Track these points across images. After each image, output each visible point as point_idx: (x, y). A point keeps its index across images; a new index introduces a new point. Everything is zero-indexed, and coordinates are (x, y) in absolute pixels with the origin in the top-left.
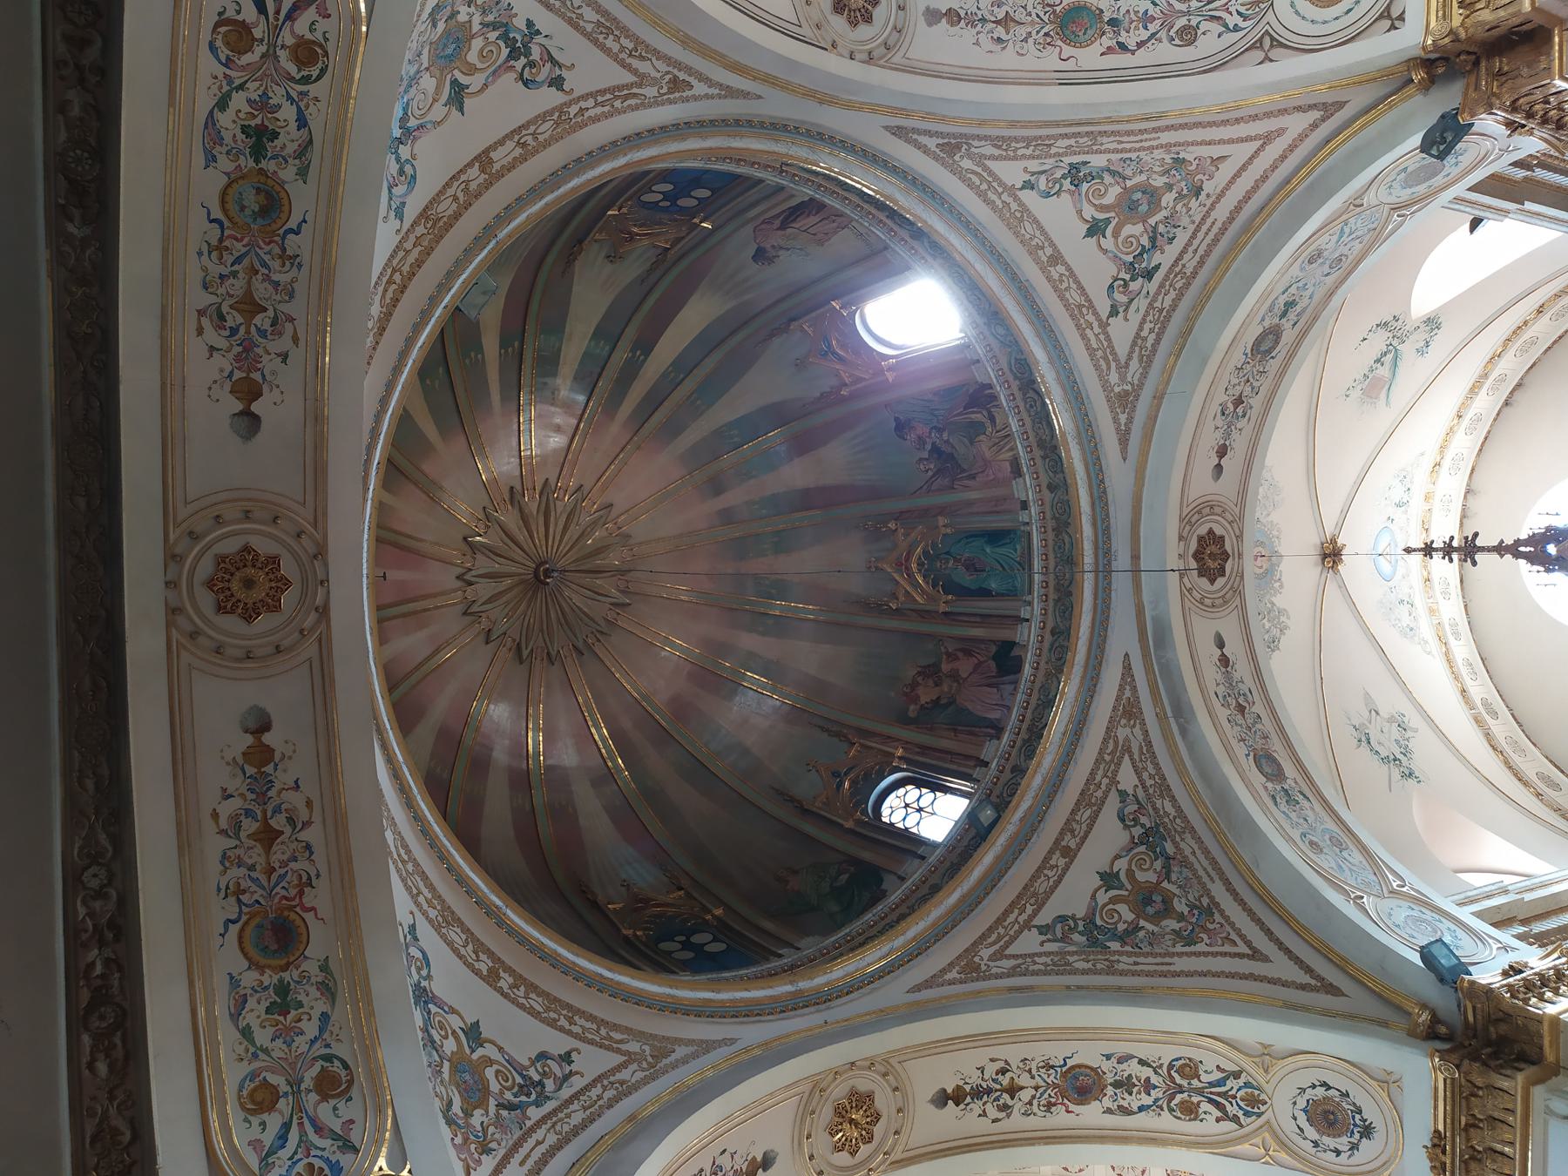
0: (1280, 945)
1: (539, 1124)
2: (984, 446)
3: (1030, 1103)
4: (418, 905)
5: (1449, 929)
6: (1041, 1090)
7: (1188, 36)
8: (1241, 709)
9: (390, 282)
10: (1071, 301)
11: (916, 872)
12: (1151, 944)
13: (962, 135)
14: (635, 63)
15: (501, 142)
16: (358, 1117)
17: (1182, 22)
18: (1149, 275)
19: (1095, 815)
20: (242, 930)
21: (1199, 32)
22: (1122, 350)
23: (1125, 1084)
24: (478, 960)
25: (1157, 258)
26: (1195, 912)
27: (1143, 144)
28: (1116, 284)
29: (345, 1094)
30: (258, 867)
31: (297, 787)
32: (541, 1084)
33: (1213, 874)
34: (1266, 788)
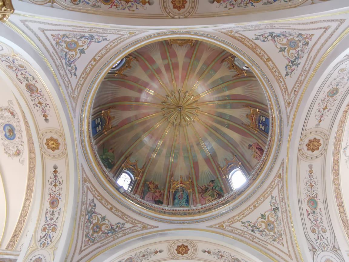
1: (61, 61)
2: (210, 198)
3: (52, 190)
4: (110, 43)
6: (54, 193)
7: (313, 231)
8: (144, 256)
9: (242, 38)
10: (245, 212)
11: (110, 175)
12: (86, 226)
13: (283, 178)
14: (293, 92)
15: (273, 63)
17: (316, 229)
18: (253, 231)
19: (120, 217)
21: (315, 233)
22: (234, 225)
23: (53, 213)
24: (98, 56)
25: (257, 232)
26: (93, 239)
27: (285, 225)
31: (137, 9)
32: (70, 66)
34: (123, 260)
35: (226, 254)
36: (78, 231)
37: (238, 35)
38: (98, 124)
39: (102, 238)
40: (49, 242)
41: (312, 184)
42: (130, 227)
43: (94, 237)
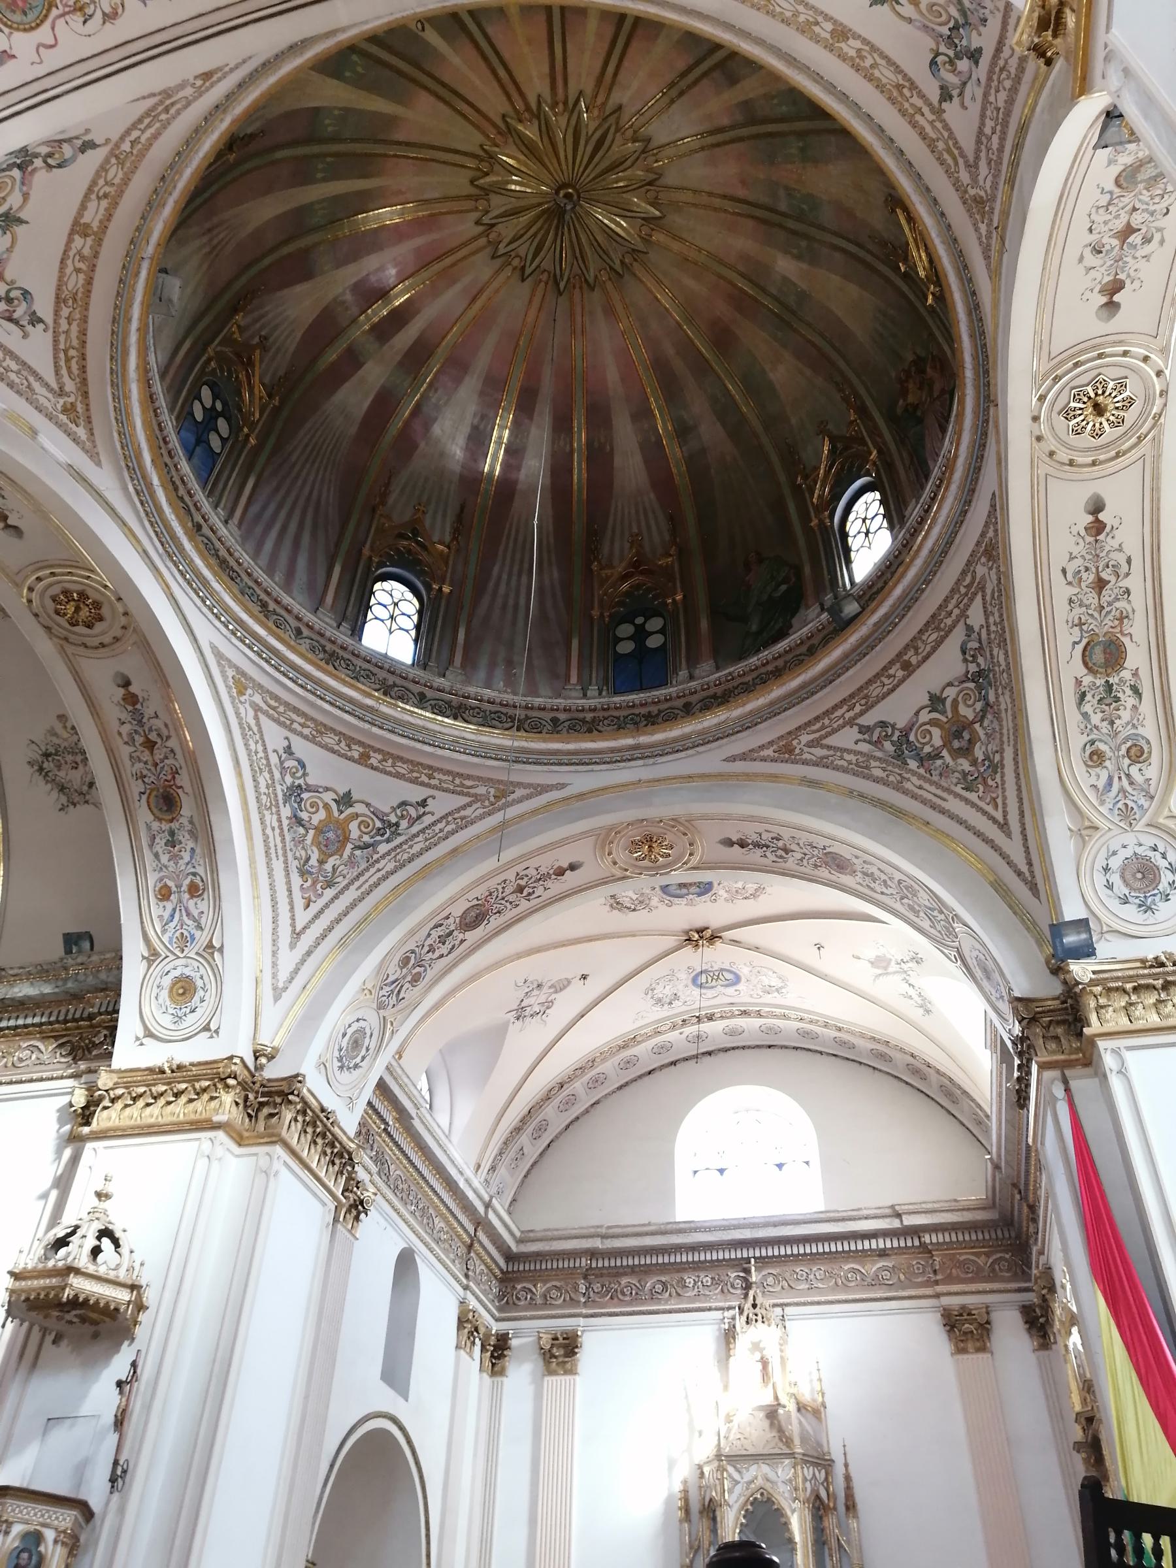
0: (1023, 830)
1: (383, 857)
3: (801, 860)
4: (294, 731)
9: (68, 360)
10: (884, 81)
12: (941, 775)
15: (83, 207)
16: (206, 912)
20: (148, 798)
22: (968, 144)
24: (350, 750)
28: (940, 59)
31: (157, 717)
32: (397, 825)
33: (1012, 737)
35: (1106, 223)
36: (943, 812)
37: (66, 379)
38: (640, 635)
42: (981, 610)
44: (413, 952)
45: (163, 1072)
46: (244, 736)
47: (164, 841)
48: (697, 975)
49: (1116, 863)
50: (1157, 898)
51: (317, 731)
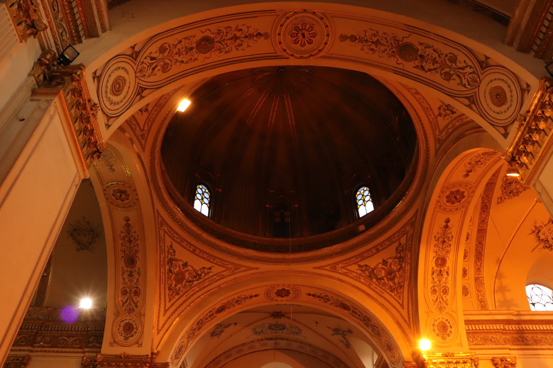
1: (195, 286)
3: (332, 303)
4: (174, 240)
5: (451, 332)
7: (448, 77)
9: (149, 121)
12: (383, 285)
17: (447, 70)
19: (390, 245)
22: (441, 127)
23: (356, 313)
26: (398, 285)
28: (442, 108)
29: (138, 296)
30: (128, 247)
31: (135, 232)
32: (201, 275)
33: (408, 279)
36: (382, 297)
39: (402, 275)
40: (378, 329)
41: (374, 41)
43: (397, 284)
44: (201, 320)
45: (121, 358)
46: (160, 240)
47: (128, 274)
48: (272, 326)
49: (436, 323)
50: (446, 335)
51: (181, 241)
